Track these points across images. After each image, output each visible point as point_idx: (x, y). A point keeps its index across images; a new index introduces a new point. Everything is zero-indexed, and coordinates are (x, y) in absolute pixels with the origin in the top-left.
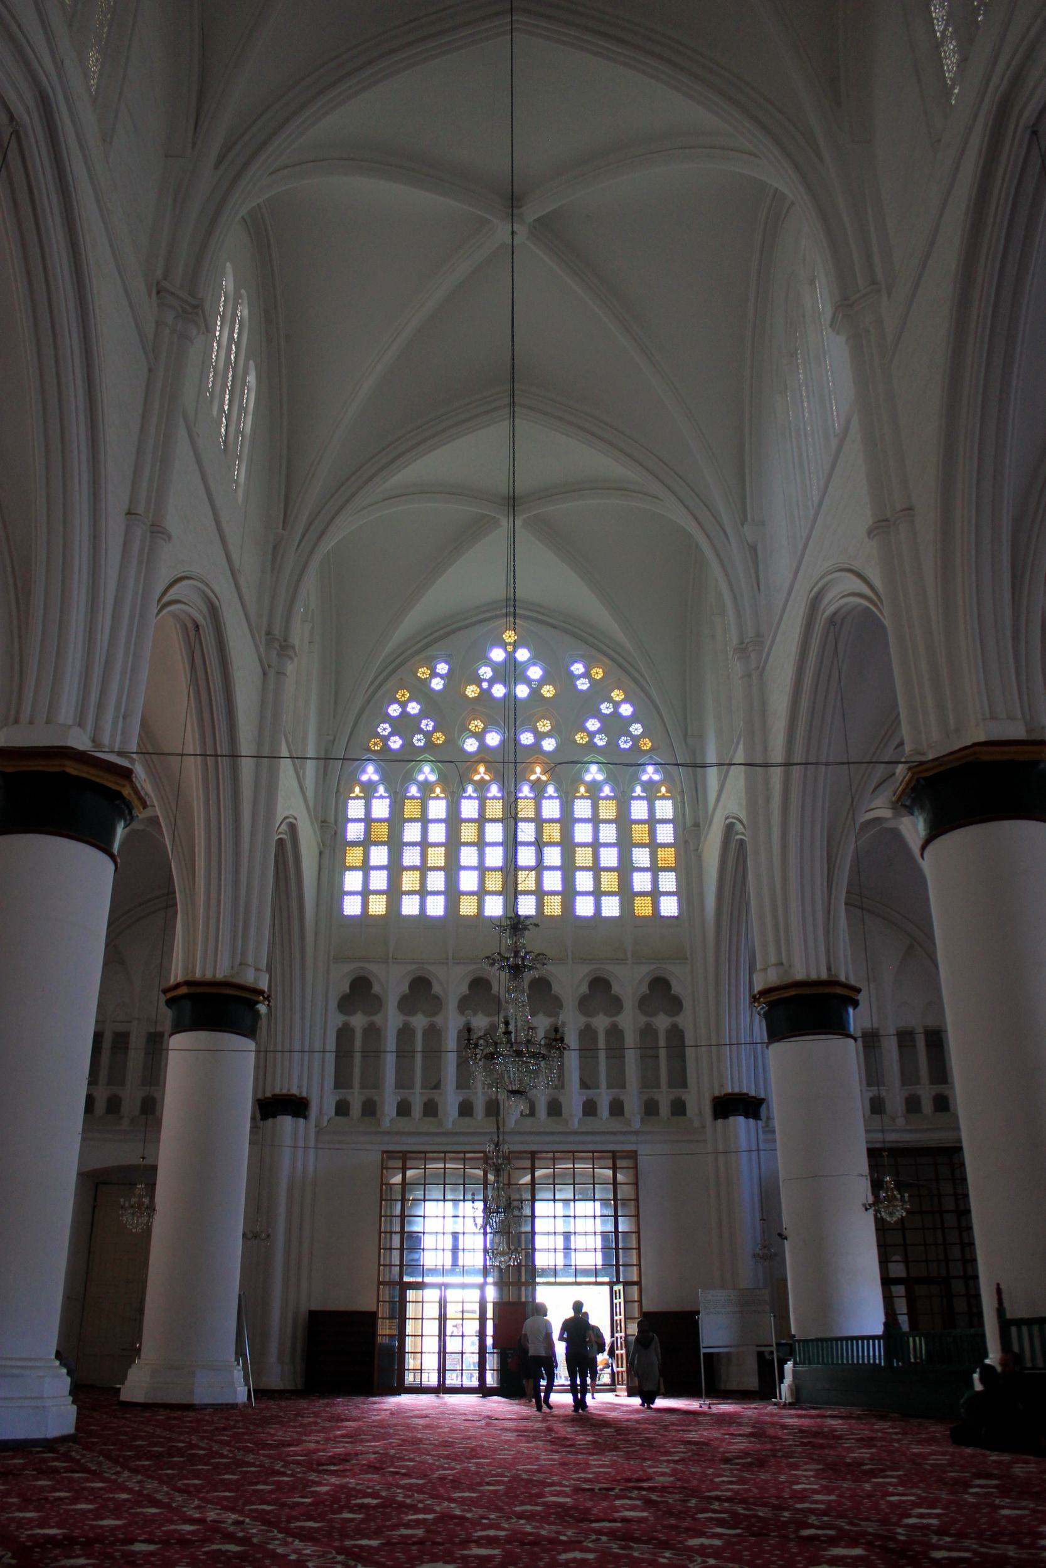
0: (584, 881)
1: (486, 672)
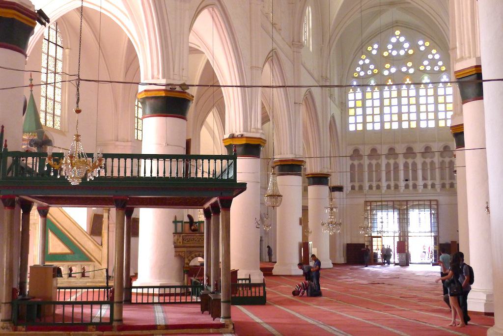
0: (423, 116)
1: (390, 47)
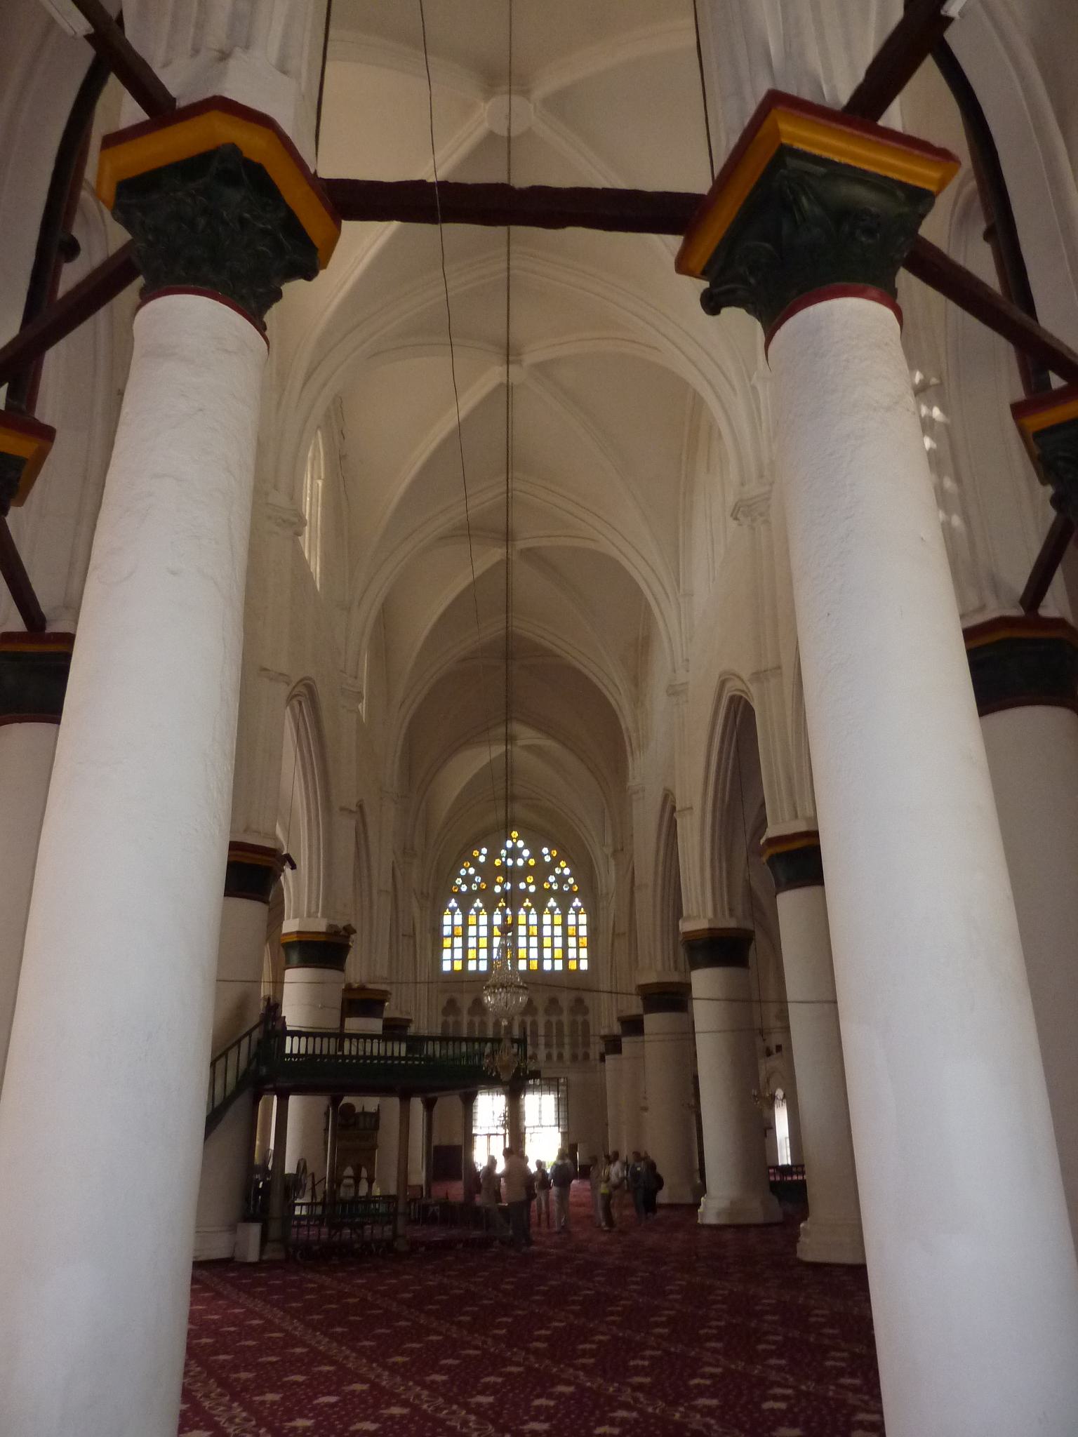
0: (547, 953)
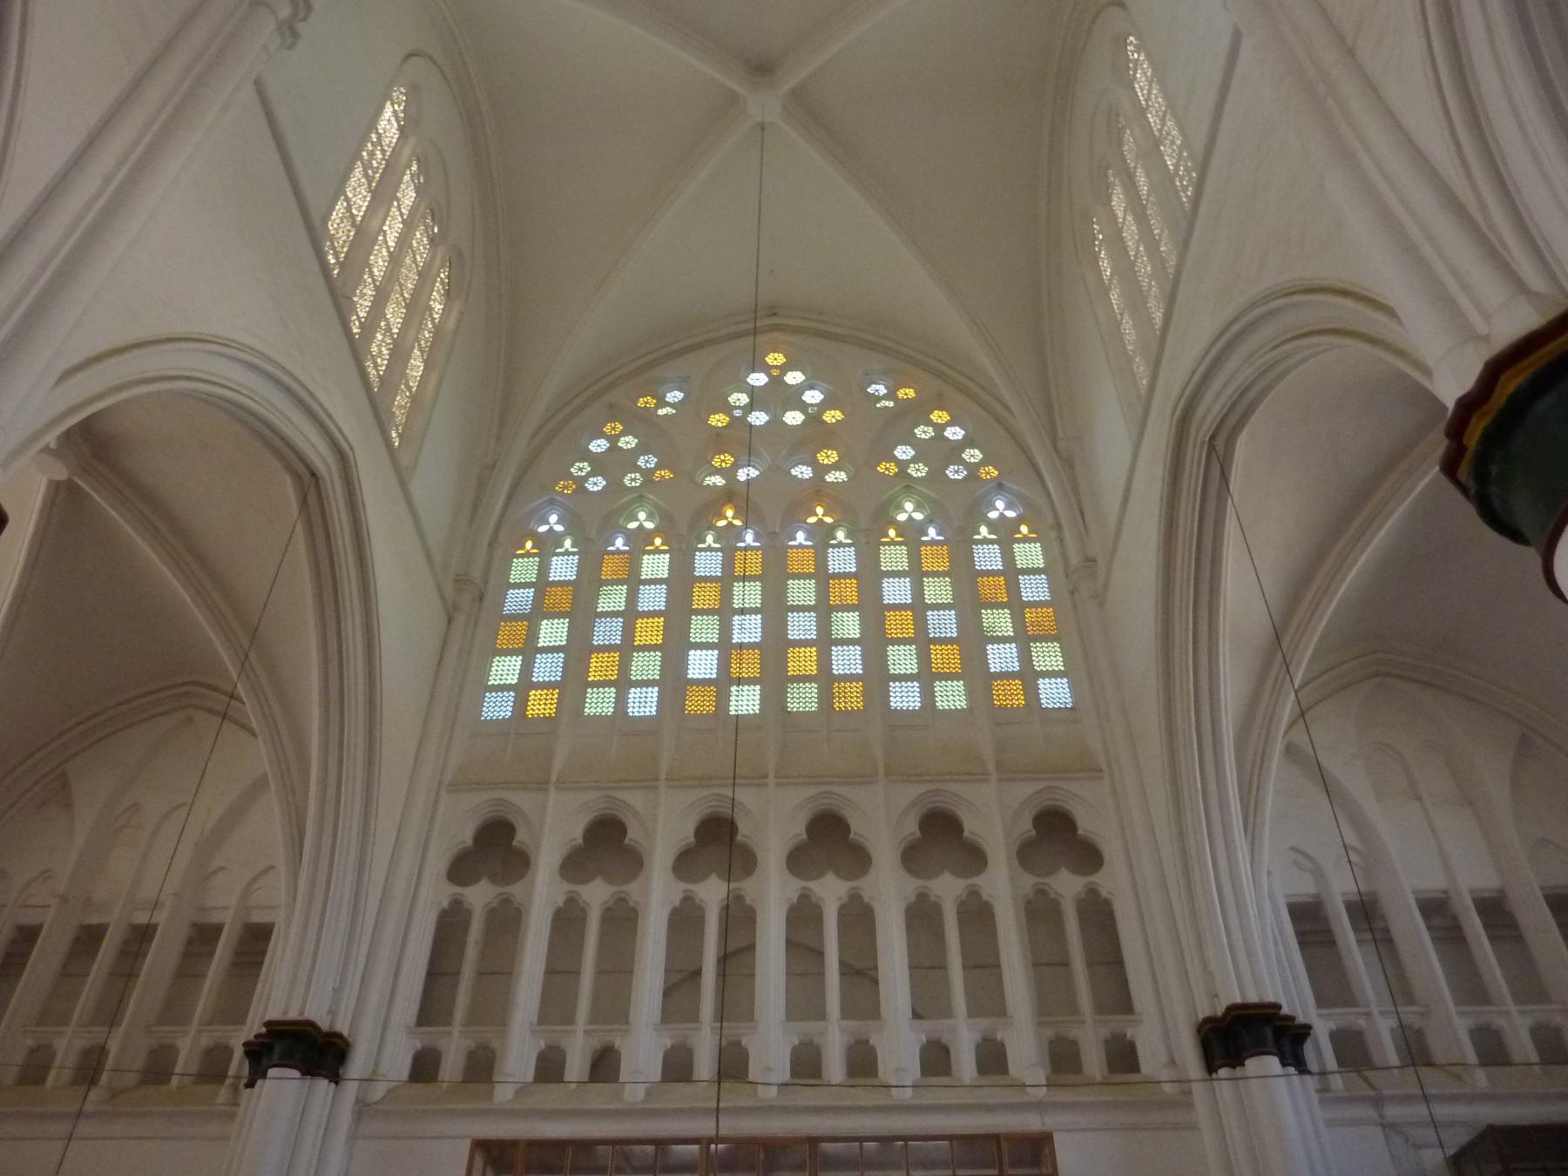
0: (902, 659)
1: (740, 398)
